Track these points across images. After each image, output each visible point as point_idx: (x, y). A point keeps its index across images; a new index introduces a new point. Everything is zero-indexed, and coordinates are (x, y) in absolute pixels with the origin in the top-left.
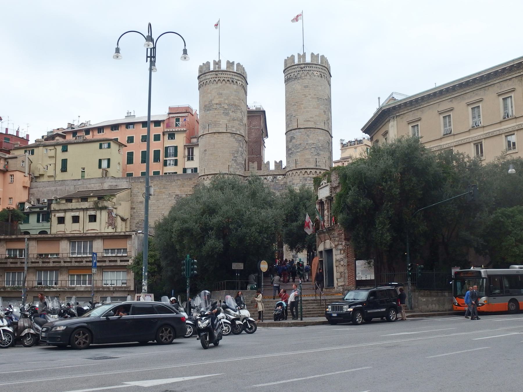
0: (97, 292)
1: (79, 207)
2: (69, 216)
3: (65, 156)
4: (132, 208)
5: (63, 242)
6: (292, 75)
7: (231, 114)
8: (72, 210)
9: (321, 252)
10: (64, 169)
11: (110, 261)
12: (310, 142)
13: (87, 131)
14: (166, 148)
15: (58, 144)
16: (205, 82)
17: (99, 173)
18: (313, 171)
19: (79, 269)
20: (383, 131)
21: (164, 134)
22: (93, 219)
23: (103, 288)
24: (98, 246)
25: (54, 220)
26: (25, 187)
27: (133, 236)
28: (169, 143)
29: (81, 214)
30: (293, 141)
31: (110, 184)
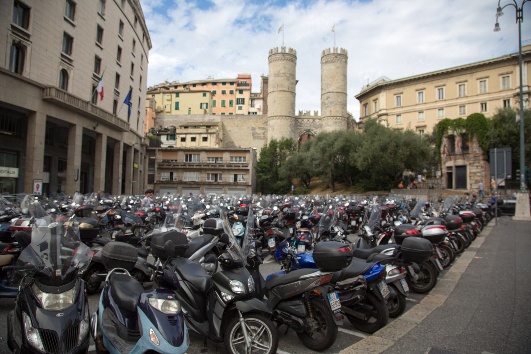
2: (189, 137)
3: (177, 99)
4: (224, 134)
8: (191, 134)
9: (450, 168)
10: (177, 108)
12: (340, 100)
14: (237, 99)
15: (173, 92)
17: (202, 111)
19: (216, 170)
20: (374, 97)
22: (205, 139)
25: (179, 140)
26: (153, 118)
28: (239, 96)
29: (197, 136)
30: (329, 99)
31: (209, 118)
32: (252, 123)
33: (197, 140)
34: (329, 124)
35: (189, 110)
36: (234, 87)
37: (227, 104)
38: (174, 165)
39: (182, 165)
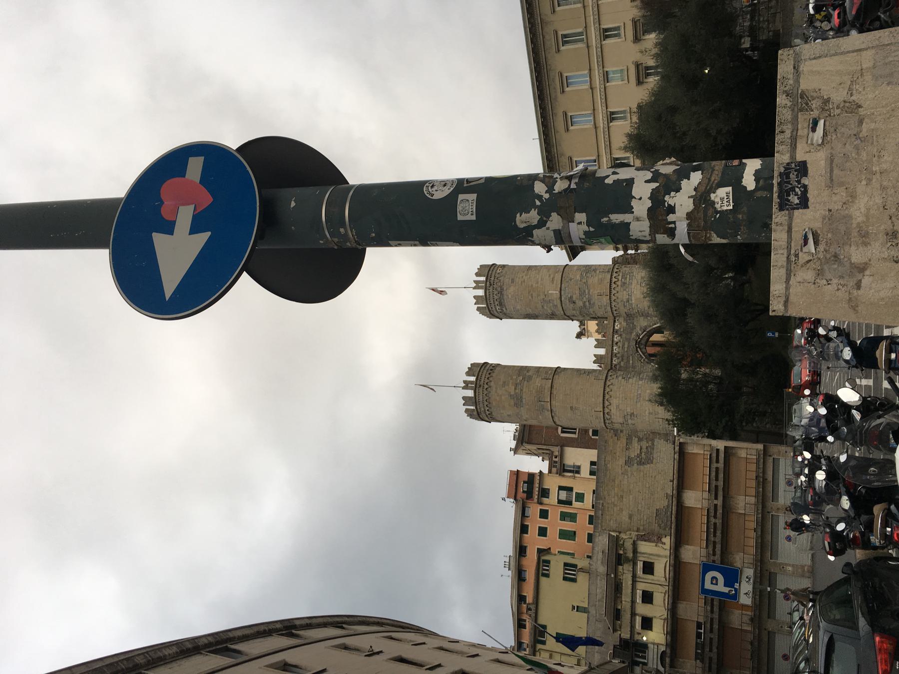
0: (764, 507)
1: (630, 591)
2: (643, 609)
5: (683, 556)
6: (496, 297)
7: (530, 373)
8: (633, 602)
11: (717, 479)
12: (578, 277)
13: (521, 599)
14: (560, 502)
16: (486, 403)
18: (615, 275)
21: (541, 503)
22: (649, 568)
23: (757, 492)
24: (695, 499)
27: (681, 440)
29: (641, 587)
31: (599, 562)
32: (617, 465)
33: (649, 588)
34: (625, 297)
35: (579, 609)
36: (534, 510)
37: (568, 526)
38: (711, 631)
39: (712, 611)
